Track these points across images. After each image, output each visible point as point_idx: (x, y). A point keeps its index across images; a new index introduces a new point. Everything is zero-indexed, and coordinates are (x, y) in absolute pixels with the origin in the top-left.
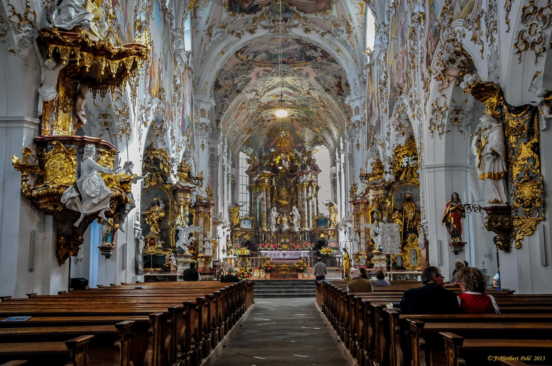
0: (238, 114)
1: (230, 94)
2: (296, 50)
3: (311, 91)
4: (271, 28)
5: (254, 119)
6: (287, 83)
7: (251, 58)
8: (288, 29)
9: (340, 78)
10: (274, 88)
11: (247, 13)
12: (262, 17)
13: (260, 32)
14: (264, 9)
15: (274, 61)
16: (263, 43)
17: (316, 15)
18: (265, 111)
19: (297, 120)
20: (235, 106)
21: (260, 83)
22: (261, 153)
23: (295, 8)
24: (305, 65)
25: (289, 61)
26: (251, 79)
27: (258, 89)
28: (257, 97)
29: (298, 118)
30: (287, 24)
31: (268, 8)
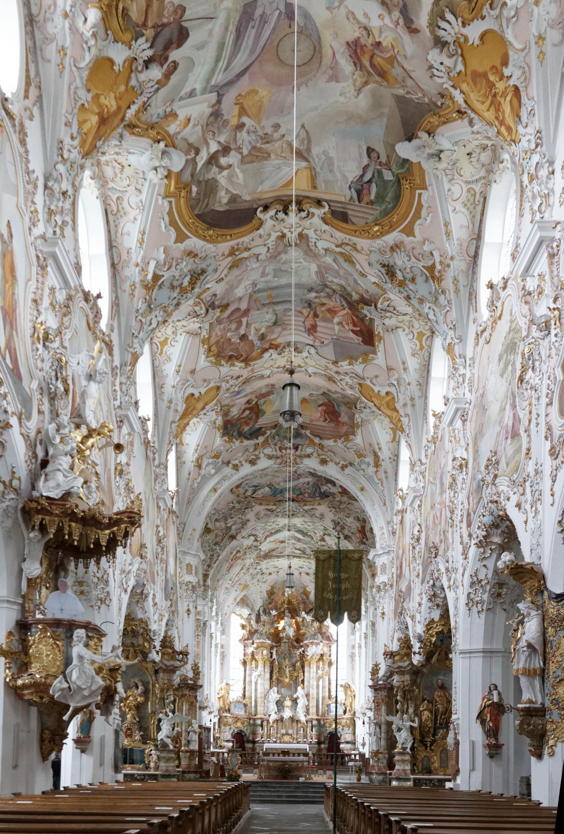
0: (231, 566)
1: (222, 540)
2: (308, 483)
3: (326, 537)
4: (278, 458)
5: (251, 571)
6: (295, 525)
7: (249, 493)
8: (298, 460)
9: (364, 521)
10: (278, 531)
11: (247, 439)
12: (266, 443)
13: (264, 463)
14: (268, 432)
15: (279, 497)
16: (266, 475)
17: (335, 441)
18: (265, 561)
19: (308, 574)
20: (227, 556)
21: (260, 525)
22: (258, 616)
23: (308, 433)
24: (319, 504)
25: (299, 497)
26: (248, 520)
27: (257, 533)
28: (255, 544)
29: (309, 571)
30: (298, 453)
31: (274, 431)
